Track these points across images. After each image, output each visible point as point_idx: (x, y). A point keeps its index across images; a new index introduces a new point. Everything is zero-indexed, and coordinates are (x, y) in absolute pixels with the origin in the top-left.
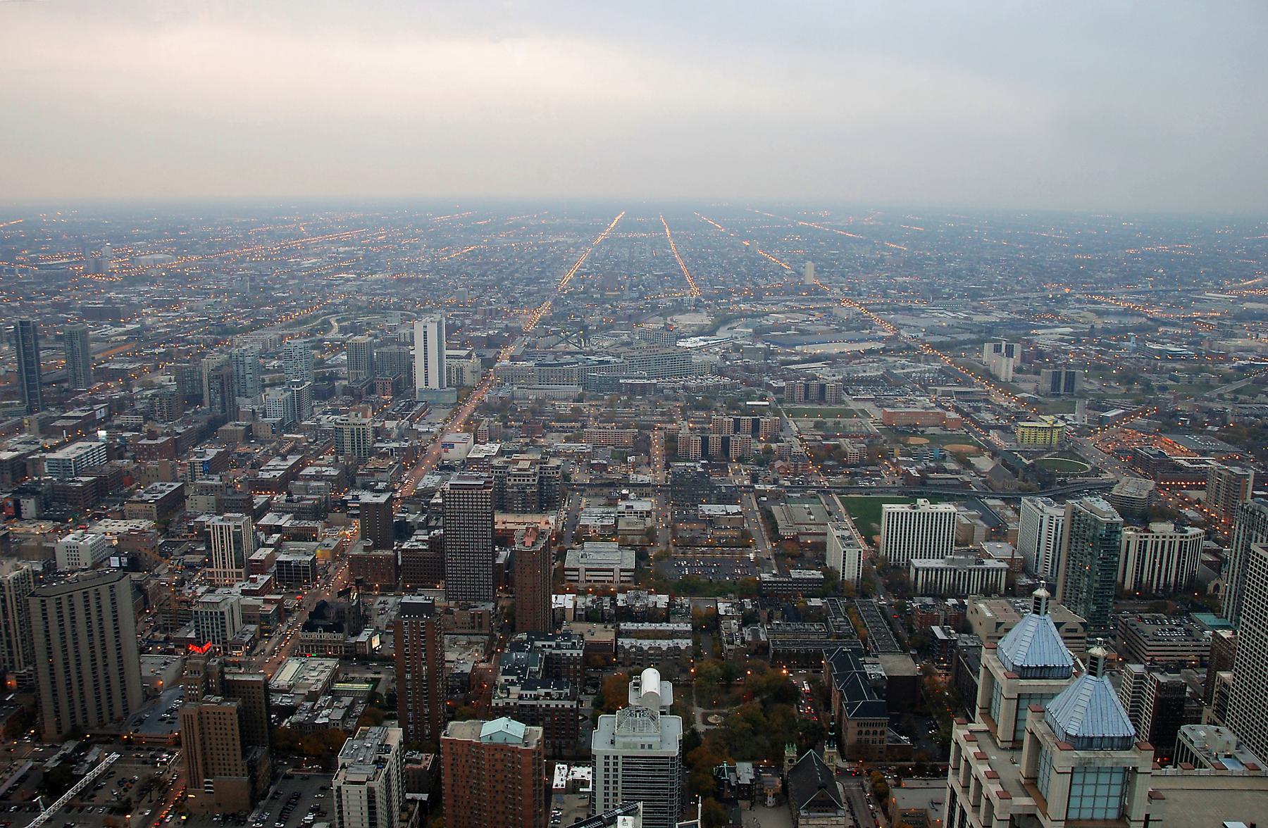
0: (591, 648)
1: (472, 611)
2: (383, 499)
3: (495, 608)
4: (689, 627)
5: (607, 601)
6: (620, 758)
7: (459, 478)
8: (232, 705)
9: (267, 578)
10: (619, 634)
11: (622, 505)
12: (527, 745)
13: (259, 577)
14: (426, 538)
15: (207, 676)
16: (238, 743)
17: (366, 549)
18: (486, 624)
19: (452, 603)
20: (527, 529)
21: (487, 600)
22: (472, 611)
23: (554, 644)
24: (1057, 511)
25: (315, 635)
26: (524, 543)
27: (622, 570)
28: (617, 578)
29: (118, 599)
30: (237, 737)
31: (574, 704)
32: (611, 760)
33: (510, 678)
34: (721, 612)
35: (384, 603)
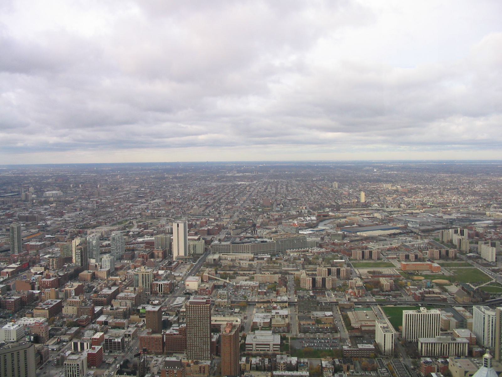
1: (200, 365)
2: (157, 309)
3: (211, 363)
5: (267, 361)
7: (194, 298)
9: (100, 347)
11: (274, 312)
13: (96, 347)
14: (178, 328)
17: (148, 333)
18: (206, 371)
19: (190, 361)
20: (227, 324)
21: (208, 359)
22: (200, 365)
24: (491, 313)
26: (225, 331)
27: (274, 345)
29: (28, 357)
34: (324, 366)
35: (157, 360)
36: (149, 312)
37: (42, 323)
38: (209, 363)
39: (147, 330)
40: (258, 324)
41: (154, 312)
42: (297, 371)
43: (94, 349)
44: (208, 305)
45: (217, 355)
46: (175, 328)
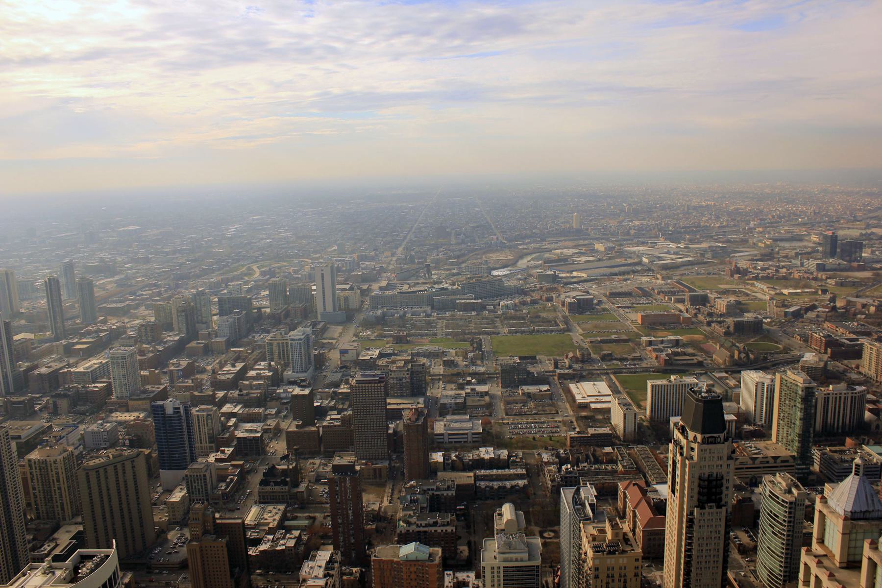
0: (460, 488)
2: (307, 392)
4: (524, 472)
6: (502, 569)
8: (223, 541)
9: (231, 449)
10: (477, 478)
11: (468, 389)
12: (432, 561)
13: (226, 449)
14: (339, 416)
15: (204, 522)
16: (227, 567)
17: (297, 426)
23: (435, 488)
25: (268, 488)
27: (473, 434)
28: (470, 439)
30: (227, 562)
31: (454, 529)
32: (496, 570)
33: (408, 513)
36: (296, 396)
37: (144, 420)
38: (386, 464)
39: (296, 423)
40: (448, 406)
41: (303, 395)
42: (509, 468)
43: (223, 452)
44: (382, 384)
45: (395, 451)
46: (333, 417)
